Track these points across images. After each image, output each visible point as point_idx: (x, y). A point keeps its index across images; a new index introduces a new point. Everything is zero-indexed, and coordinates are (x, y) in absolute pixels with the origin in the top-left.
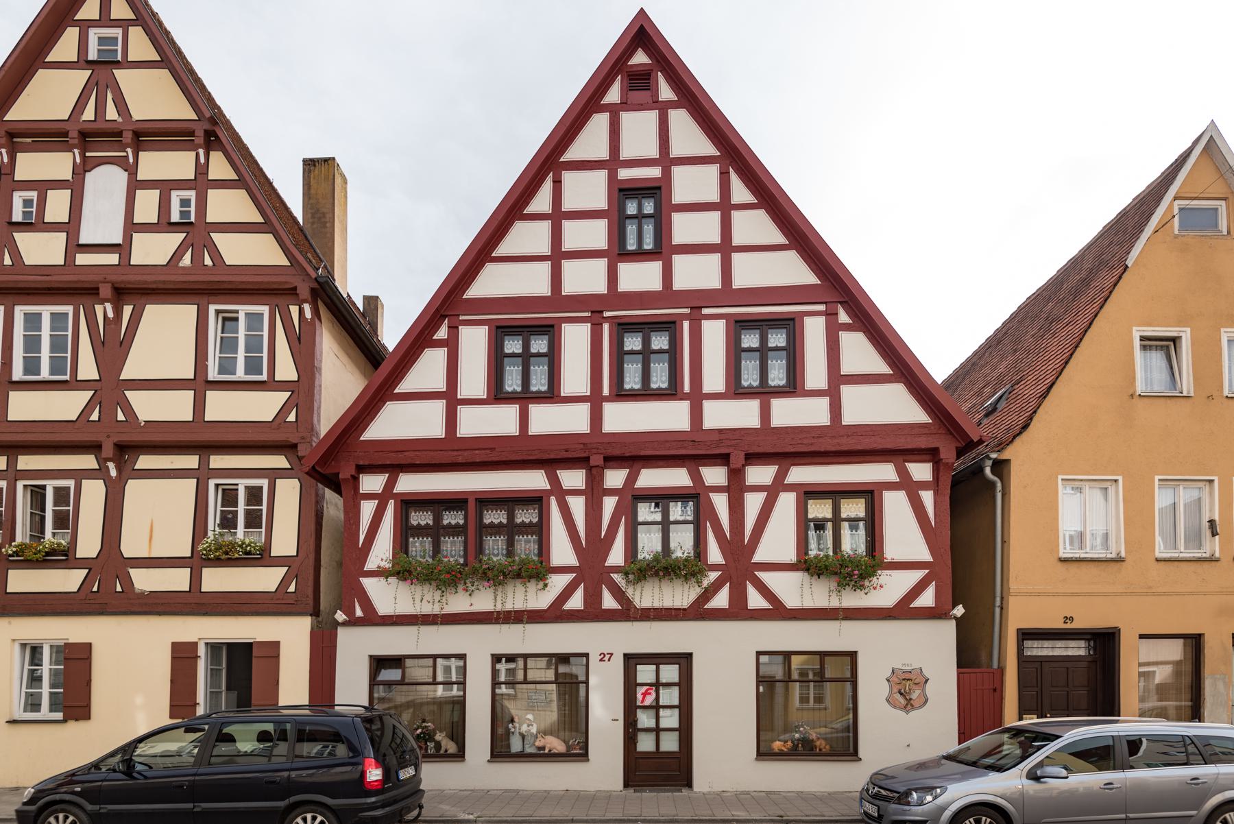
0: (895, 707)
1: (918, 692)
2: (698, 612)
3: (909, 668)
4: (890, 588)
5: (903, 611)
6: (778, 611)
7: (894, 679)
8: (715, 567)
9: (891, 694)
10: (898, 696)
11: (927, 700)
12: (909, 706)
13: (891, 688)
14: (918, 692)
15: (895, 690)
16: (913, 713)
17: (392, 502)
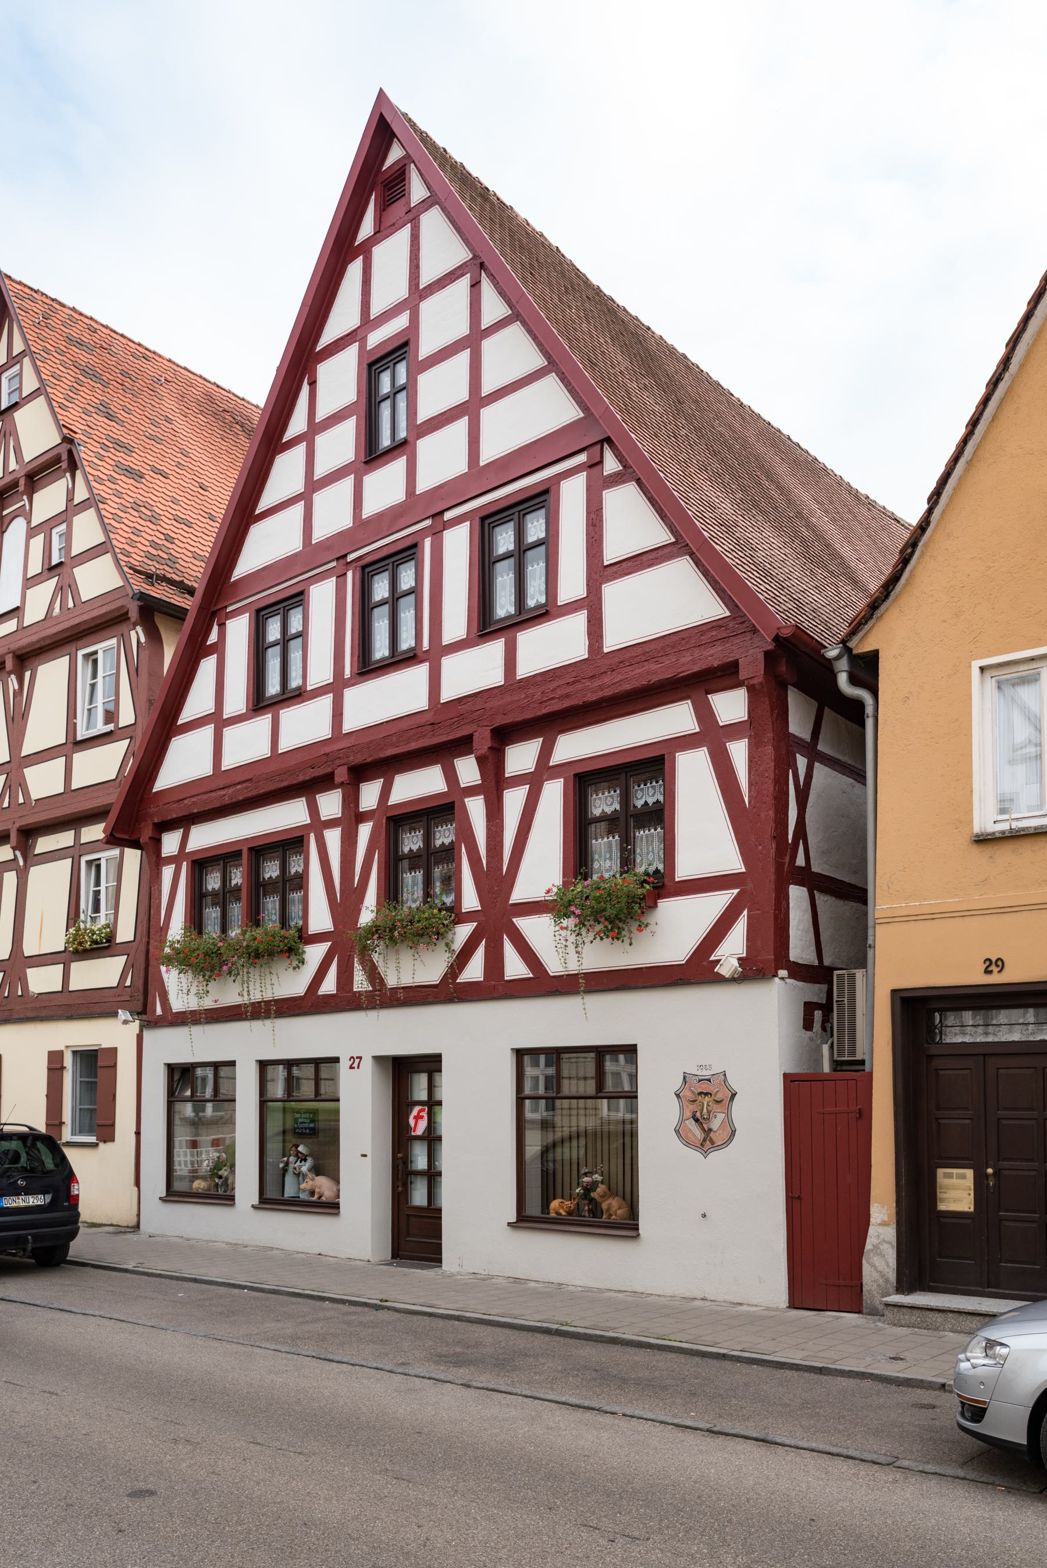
0: (687, 1144)
1: (721, 1117)
2: (449, 991)
3: (706, 1073)
4: (677, 928)
5: (698, 970)
6: (541, 985)
7: (687, 1094)
8: (470, 916)
9: (682, 1120)
10: (691, 1124)
11: (733, 1133)
12: (707, 1143)
13: (682, 1109)
14: (721, 1117)
15: (688, 1114)
16: (714, 1156)
17: (185, 863)
